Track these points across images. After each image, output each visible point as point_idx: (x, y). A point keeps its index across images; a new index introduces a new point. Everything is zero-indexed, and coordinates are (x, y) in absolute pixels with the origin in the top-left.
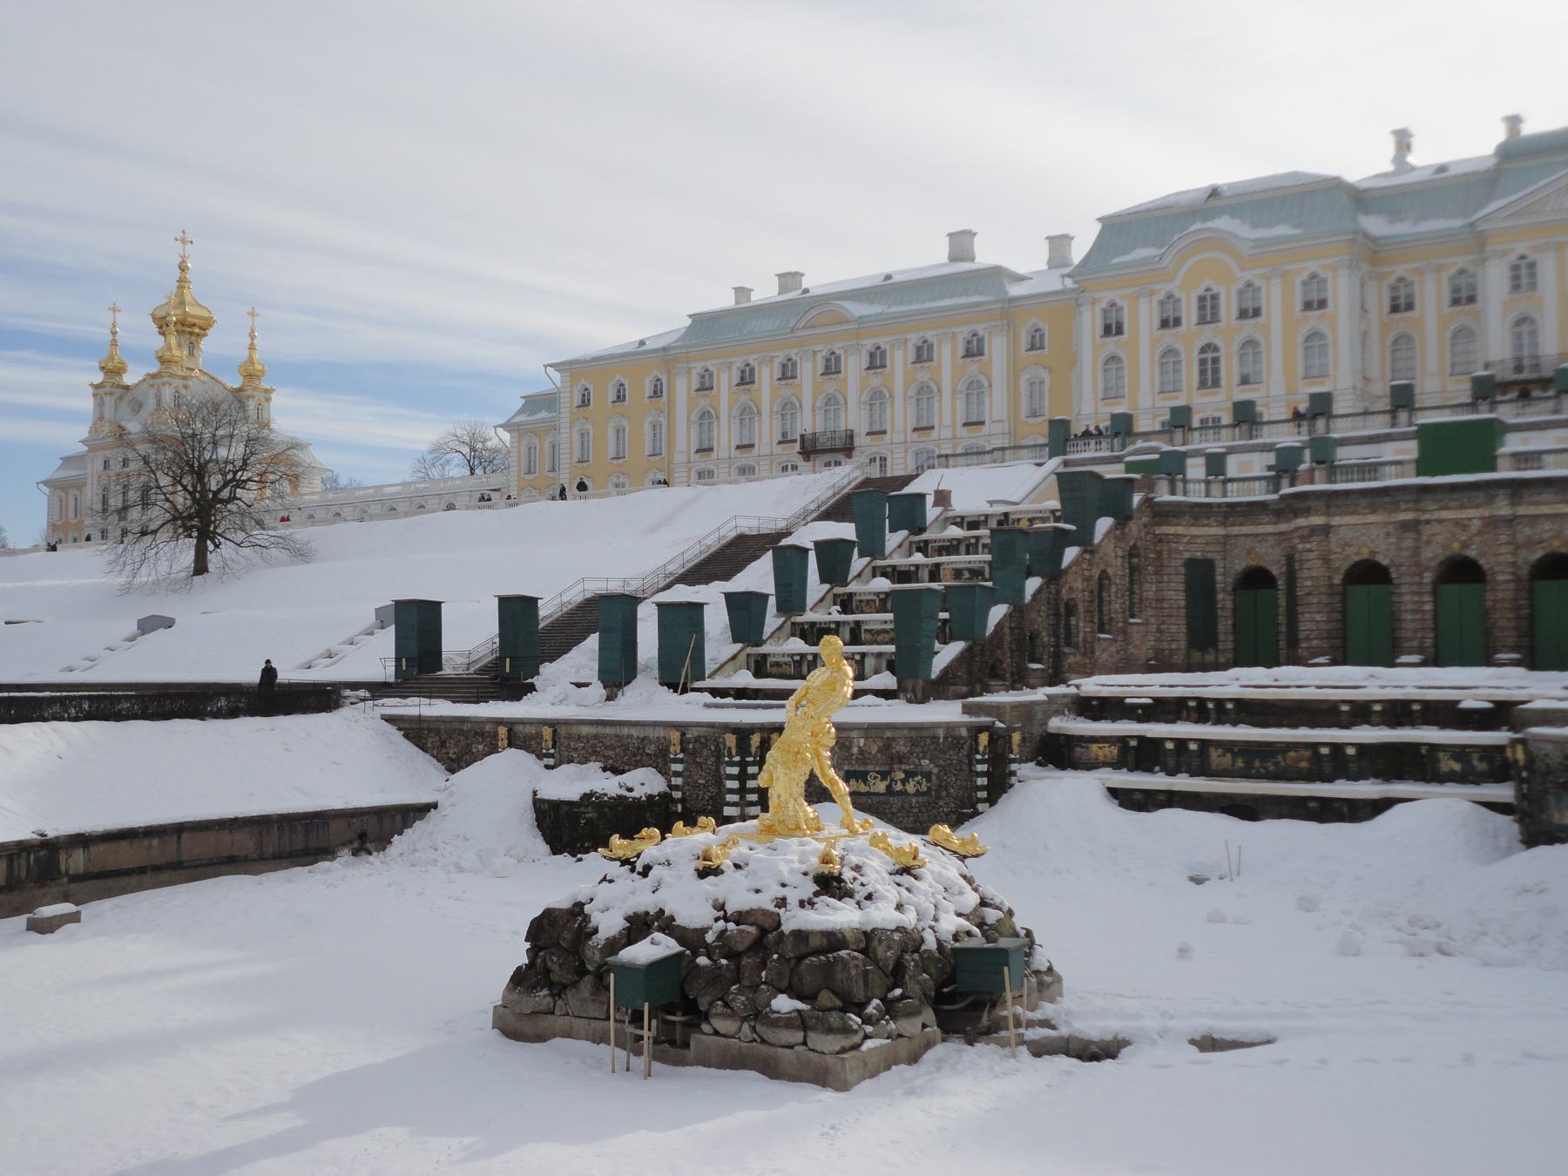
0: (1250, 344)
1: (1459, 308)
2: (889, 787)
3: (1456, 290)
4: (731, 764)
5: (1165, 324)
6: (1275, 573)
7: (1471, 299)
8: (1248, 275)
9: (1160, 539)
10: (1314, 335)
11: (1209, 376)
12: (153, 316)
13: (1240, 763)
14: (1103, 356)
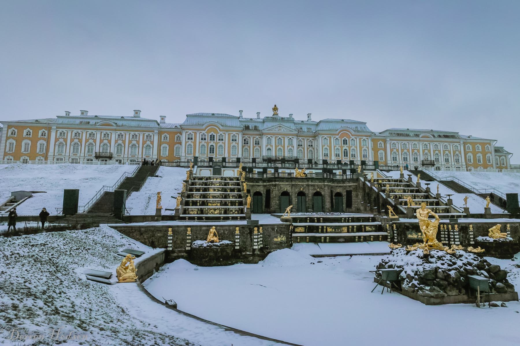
3: (256, 142)
4: (255, 235)
5: (202, 139)
6: (262, 192)
7: (258, 144)
14: (187, 144)
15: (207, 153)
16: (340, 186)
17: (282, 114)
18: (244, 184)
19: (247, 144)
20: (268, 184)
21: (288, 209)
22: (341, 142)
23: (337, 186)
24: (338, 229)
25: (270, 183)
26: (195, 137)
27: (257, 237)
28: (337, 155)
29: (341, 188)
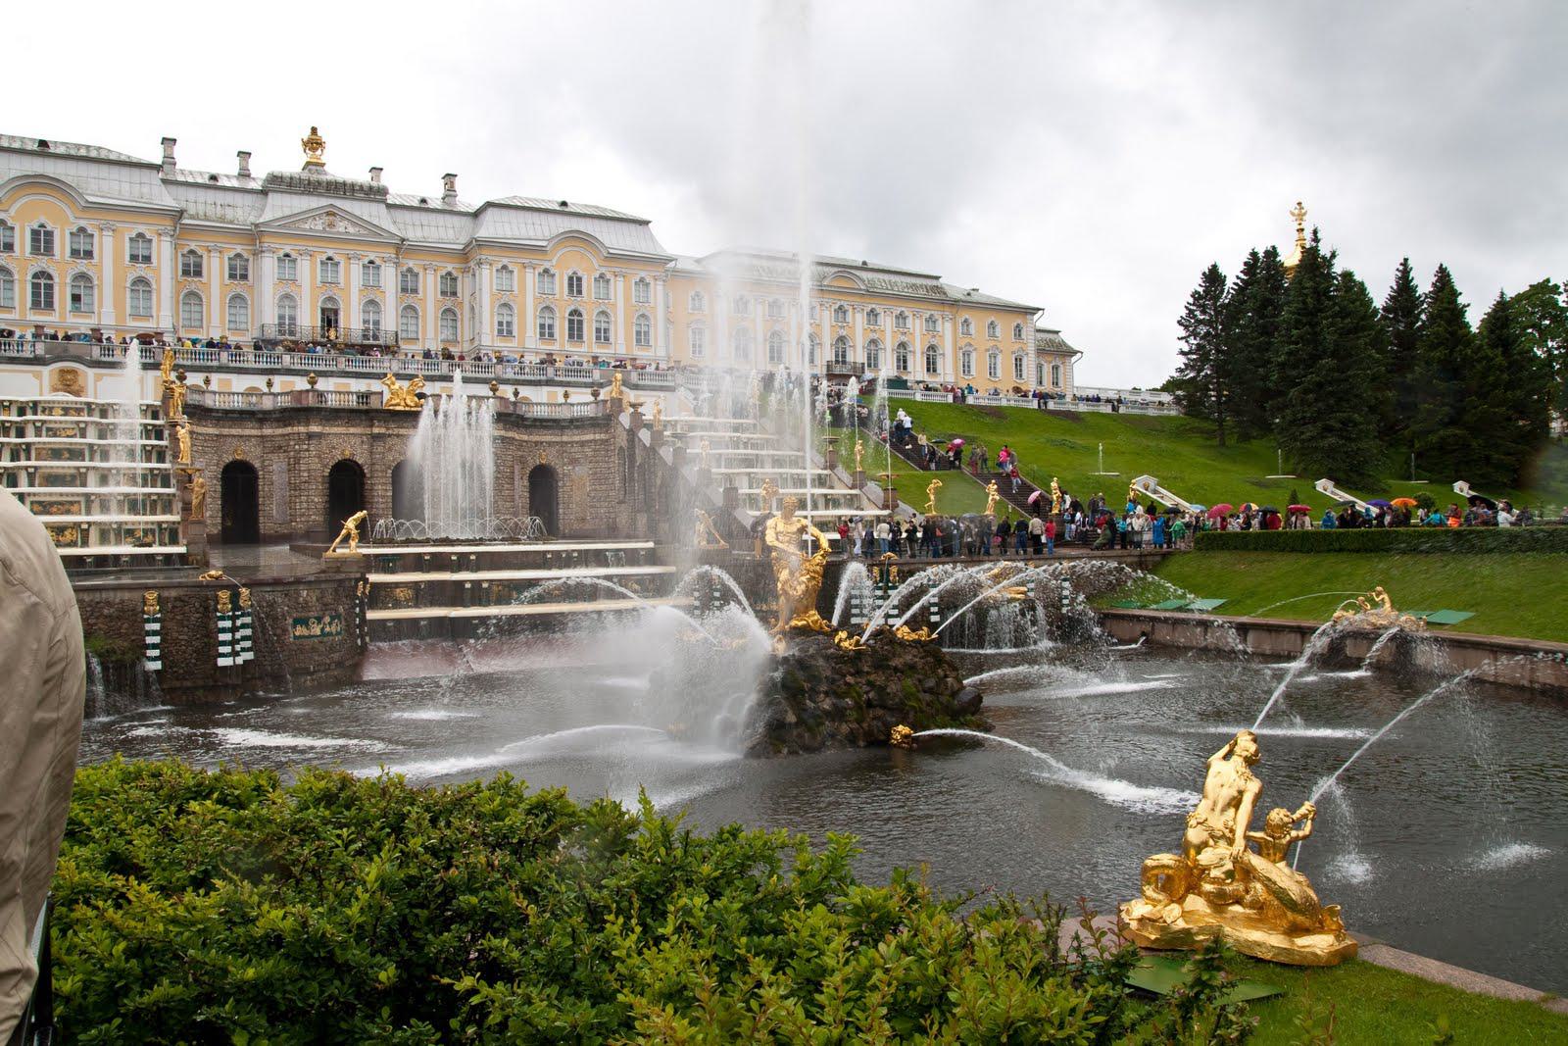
0: (82, 277)
2: (322, 629)
3: (232, 268)
4: (223, 618)
6: (257, 464)
7: (244, 277)
8: (83, 223)
10: (141, 281)
16: (550, 444)
17: (343, 164)
18: (182, 432)
19: (198, 273)
20: (280, 431)
21: (350, 524)
22: (561, 285)
23: (536, 443)
25: (289, 430)
27: (228, 624)
28: (546, 332)
29: (553, 450)
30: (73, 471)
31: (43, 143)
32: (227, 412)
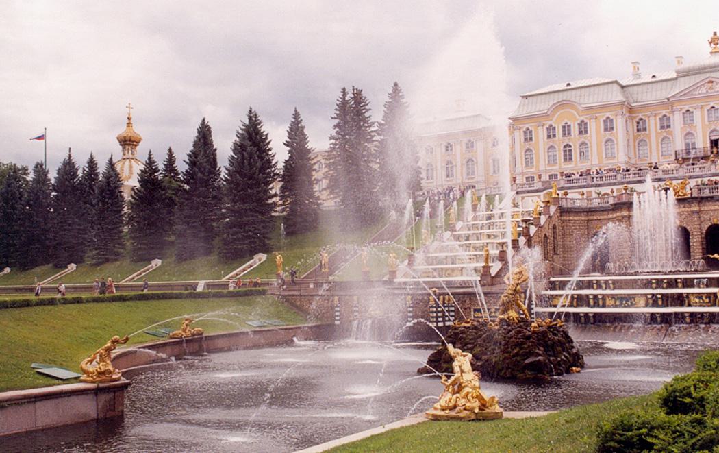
0: (583, 143)
1: (663, 130)
5: (549, 137)
8: (582, 118)
9: (563, 222)
11: (568, 157)
12: (118, 138)
13: (618, 303)
15: (560, 161)
24: (627, 301)
26: (537, 133)
30: (482, 245)
31: (569, 85)
32: (590, 208)
